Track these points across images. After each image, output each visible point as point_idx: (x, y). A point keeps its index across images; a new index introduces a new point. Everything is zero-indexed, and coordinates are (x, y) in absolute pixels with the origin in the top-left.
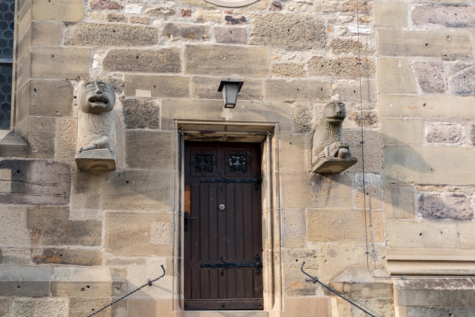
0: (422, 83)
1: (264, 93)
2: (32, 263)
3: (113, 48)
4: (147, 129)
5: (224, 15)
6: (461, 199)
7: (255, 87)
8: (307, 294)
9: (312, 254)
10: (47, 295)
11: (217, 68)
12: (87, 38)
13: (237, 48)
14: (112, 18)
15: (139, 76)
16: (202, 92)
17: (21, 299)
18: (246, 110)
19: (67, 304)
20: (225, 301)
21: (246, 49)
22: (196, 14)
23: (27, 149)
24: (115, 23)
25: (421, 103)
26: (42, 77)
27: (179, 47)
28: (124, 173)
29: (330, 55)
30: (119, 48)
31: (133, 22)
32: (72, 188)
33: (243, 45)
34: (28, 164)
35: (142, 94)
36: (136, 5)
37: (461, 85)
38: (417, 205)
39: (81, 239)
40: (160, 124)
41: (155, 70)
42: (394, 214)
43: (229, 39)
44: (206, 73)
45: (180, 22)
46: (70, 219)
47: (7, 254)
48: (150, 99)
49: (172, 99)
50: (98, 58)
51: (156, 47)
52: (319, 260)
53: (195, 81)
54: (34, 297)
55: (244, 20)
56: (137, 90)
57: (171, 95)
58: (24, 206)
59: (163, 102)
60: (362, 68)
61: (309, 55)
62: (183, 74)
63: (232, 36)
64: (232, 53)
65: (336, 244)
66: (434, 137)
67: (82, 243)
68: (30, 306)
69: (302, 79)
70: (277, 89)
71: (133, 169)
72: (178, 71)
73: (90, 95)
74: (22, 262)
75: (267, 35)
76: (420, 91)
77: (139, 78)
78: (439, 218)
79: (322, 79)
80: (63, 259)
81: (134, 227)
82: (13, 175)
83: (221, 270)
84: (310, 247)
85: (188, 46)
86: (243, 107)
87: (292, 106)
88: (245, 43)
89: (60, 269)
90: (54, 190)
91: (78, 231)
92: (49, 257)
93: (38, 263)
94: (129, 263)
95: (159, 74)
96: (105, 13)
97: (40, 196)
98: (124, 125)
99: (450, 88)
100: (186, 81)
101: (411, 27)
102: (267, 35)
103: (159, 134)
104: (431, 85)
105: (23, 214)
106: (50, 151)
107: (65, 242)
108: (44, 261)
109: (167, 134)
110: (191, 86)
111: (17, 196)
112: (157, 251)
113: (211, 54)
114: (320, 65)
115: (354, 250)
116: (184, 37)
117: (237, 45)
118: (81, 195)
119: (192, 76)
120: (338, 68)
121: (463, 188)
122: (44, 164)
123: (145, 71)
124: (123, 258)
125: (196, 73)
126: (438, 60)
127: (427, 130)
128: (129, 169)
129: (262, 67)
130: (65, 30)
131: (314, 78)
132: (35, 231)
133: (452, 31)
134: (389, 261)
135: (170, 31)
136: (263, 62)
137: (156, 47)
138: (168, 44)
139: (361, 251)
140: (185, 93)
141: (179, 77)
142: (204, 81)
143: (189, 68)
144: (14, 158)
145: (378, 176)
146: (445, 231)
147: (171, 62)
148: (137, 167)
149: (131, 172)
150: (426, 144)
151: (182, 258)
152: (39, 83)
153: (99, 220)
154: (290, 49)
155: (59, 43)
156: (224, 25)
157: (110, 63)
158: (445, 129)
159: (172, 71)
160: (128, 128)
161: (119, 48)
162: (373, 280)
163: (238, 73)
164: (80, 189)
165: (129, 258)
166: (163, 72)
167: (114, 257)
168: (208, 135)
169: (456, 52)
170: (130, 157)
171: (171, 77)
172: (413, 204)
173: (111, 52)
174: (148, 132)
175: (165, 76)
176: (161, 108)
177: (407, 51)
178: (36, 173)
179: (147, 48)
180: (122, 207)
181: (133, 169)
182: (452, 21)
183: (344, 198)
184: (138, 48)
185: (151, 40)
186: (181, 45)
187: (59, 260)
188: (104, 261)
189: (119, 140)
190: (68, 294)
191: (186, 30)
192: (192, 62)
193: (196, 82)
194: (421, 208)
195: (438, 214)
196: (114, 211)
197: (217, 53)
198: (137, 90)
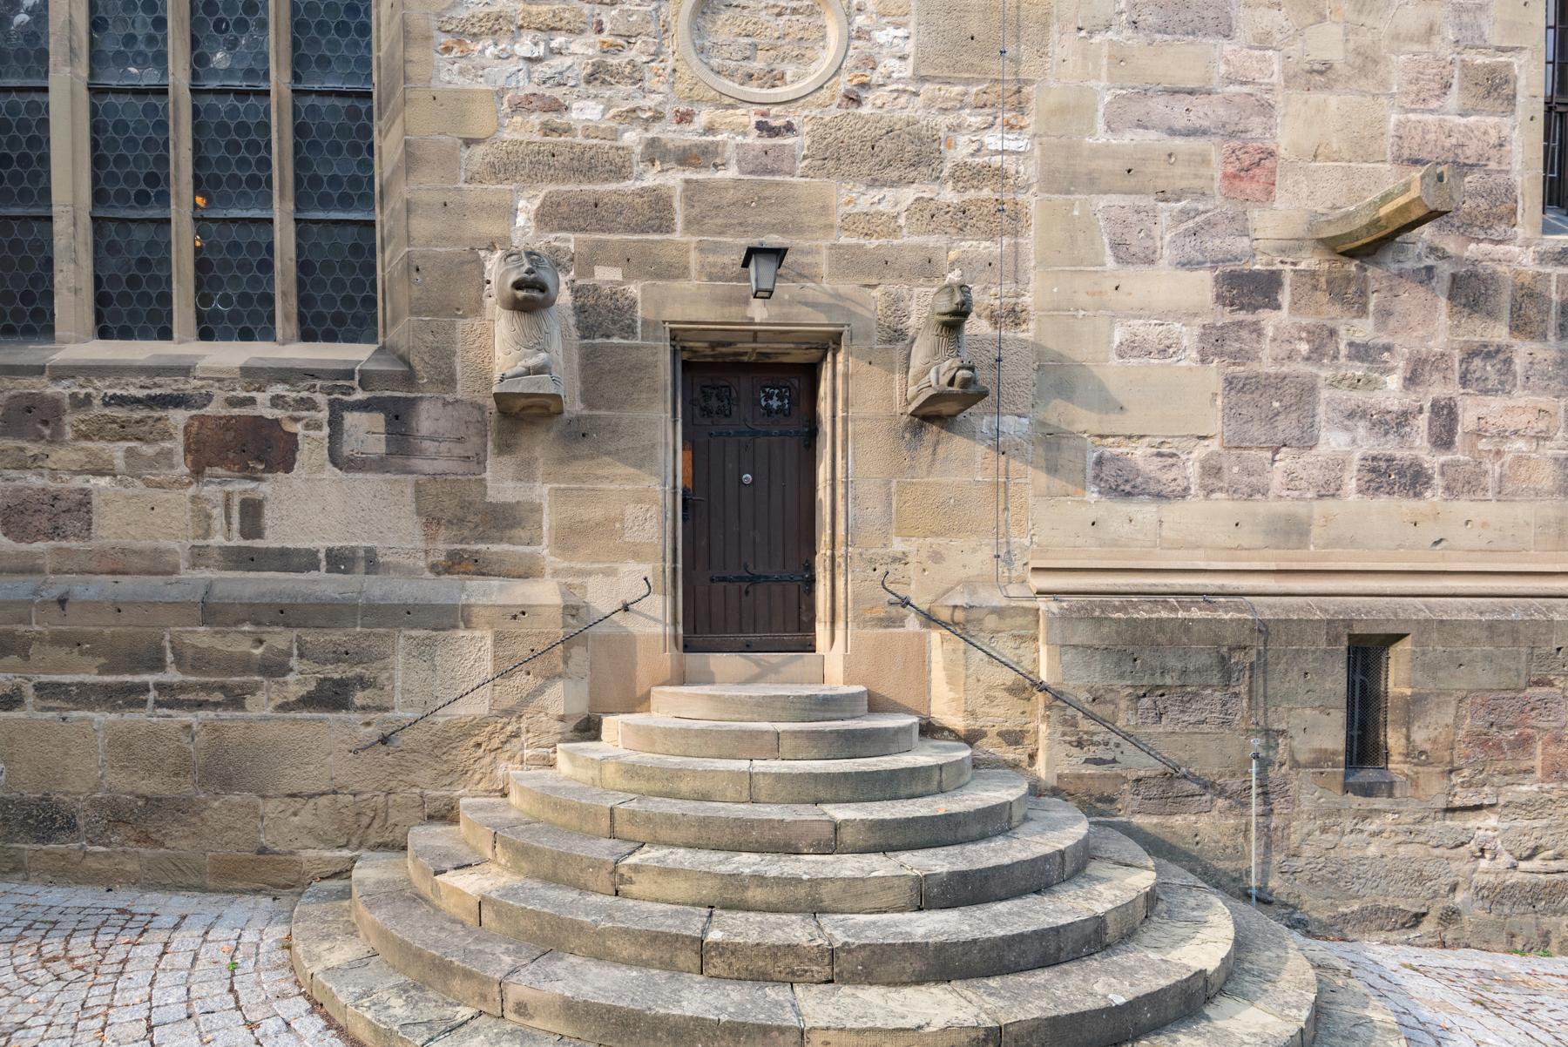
0: (1116, 245)
1: (824, 270)
2: (428, 574)
3: (552, 187)
4: (615, 340)
5: (754, 119)
6: (1170, 461)
9: (902, 559)
10: (455, 627)
11: (740, 224)
12: (505, 168)
13: (778, 184)
14: (548, 129)
15: (600, 241)
16: (714, 270)
17: (414, 633)
18: (791, 302)
19: (489, 642)
20: (752, 637)
21: (793, 186)
22: (703, 117)
23: (409, 378)
24: (554, 138)
25: (1109, 285)
26: (428, 243)
27: (671, 183)
28: (578, 419)
29: (949, 195)
30: (563, 188)
31: (587, 137)
32: (490, 446)
33: (788, 179)
34: (411, 403)
35: (606, 275)
36: (591, 103)
37: (1188, 249)
38: (1090, 473)
39: (508, 533)
40: (639, 330)
41: (628, 228)
43: (763, 165)
44: (721, 233)
45: (671, 134)
46: (488, 500)
47: (386, 559)
48: (620, 284)
50: (527, 207)
51: (630, 185)
52: (912, 570)
53: (701, 249)
54: (435, 629)
55: (789, 128)
56: (596, 268)
57: (658, 276)
58: (410, 477)
59: (643, 290)
60: (1008, 219)
61: (908, 195)
62: (677, 236)
63: (768, 161)
64: (767, 193)
65: (943, 541)
66: (1130, 348)
67: (510, 541)
68: (430, 644)
69: (895, 242)
70: (849, 261)
73: (513, 277)
74: (412, 573)
75: (834, 156)
76: (1110, 262)
77: (601, 245)
78: (1129, 494)
79: (932, 241)
80: (480, 567)
81: (597, 513)
82: (388, 423)
84: (898, 546)
85: (687, 181)
87: (876, 293)
88: (792, 174)
89: (475, 584)
90: (458, 450)
91: (503, 520)
92: (455, 564)
93: (438, 574)
94: (589, 574)
95: (636, 237)
96: (536, 119)
97: (435, 460)
98: (575, 333)
99: (1167, 254)
100: (683, 250)
101: (1101, 137)
102: (834, 156)
103: (638, 348)
104: (1132, 250)
105: (409, 491)
106: (449, 381)
107: (482, 539)
108: (448, 570)
110: (694, 258)
111: (397, 460)
112: (636, 554)
113: (730, 195)
114: (927, 214)
115: (974, 551)
116: (681, 165)
117: (777, 178)
118: (506, 459)
121: (1176, 442)
122: (440, 404)
123: (610, 231)
124: (579, 566)
125: (702, 233)
126: (1147, 201)
127: (1118, 335)
128: (585, 412)
129: (822, 221)
130: (465, 153)
132: (431, 521)
133: (1179, 142)
134: (1034, 569)
135: (655, 152)
136: (825, 209)
137: (630, 185)
138: (652, 178)
139: (986, 553)
140: (681, 272)
141: (671, 242)
142: (716, 248)
143: (689, 223)
144: (388, 393)
145: (1024, 420)
146: (1138, 517)
147: (657, 213)
148: (599, 408)
149: (591, 417)
150: (1115, 361)
151: (680, 566)
152: (423, 256)
154: (874, 183)
155: (455, 180)
156: (754, 139)
157: (548, 216)
158: (1150, 332)
159: (659, 230)
160: (583, 337)
161: (563, 188)
162: (1004, 603)
163: (778, 232)
164: (504, 448)
165: (589, 567)
166: (642, 232)
167: (566, 564)
168: (724, 350)
169: (1184, 184)
170: (587, 390)
172: (1084, 470)
173: (549, 195)
174: (618, 346)
175: (647, 241)
177: (1093, 184)
178: (427, 420)
179: (613, 186)
180: (575, 478)
182: (1181, 123)
183: (962, 461)
184: (597, 188)
185: (619, 171)
186: (675, 179)
187: (472, 568)
188: (548, 570)
189: (568, 360)
190: (491, 624)
191: (685, 150)
193: (702, 250)
194: (1096, 477)
195: (1128, 488)
197: (740, 195)
198: (596, 268)
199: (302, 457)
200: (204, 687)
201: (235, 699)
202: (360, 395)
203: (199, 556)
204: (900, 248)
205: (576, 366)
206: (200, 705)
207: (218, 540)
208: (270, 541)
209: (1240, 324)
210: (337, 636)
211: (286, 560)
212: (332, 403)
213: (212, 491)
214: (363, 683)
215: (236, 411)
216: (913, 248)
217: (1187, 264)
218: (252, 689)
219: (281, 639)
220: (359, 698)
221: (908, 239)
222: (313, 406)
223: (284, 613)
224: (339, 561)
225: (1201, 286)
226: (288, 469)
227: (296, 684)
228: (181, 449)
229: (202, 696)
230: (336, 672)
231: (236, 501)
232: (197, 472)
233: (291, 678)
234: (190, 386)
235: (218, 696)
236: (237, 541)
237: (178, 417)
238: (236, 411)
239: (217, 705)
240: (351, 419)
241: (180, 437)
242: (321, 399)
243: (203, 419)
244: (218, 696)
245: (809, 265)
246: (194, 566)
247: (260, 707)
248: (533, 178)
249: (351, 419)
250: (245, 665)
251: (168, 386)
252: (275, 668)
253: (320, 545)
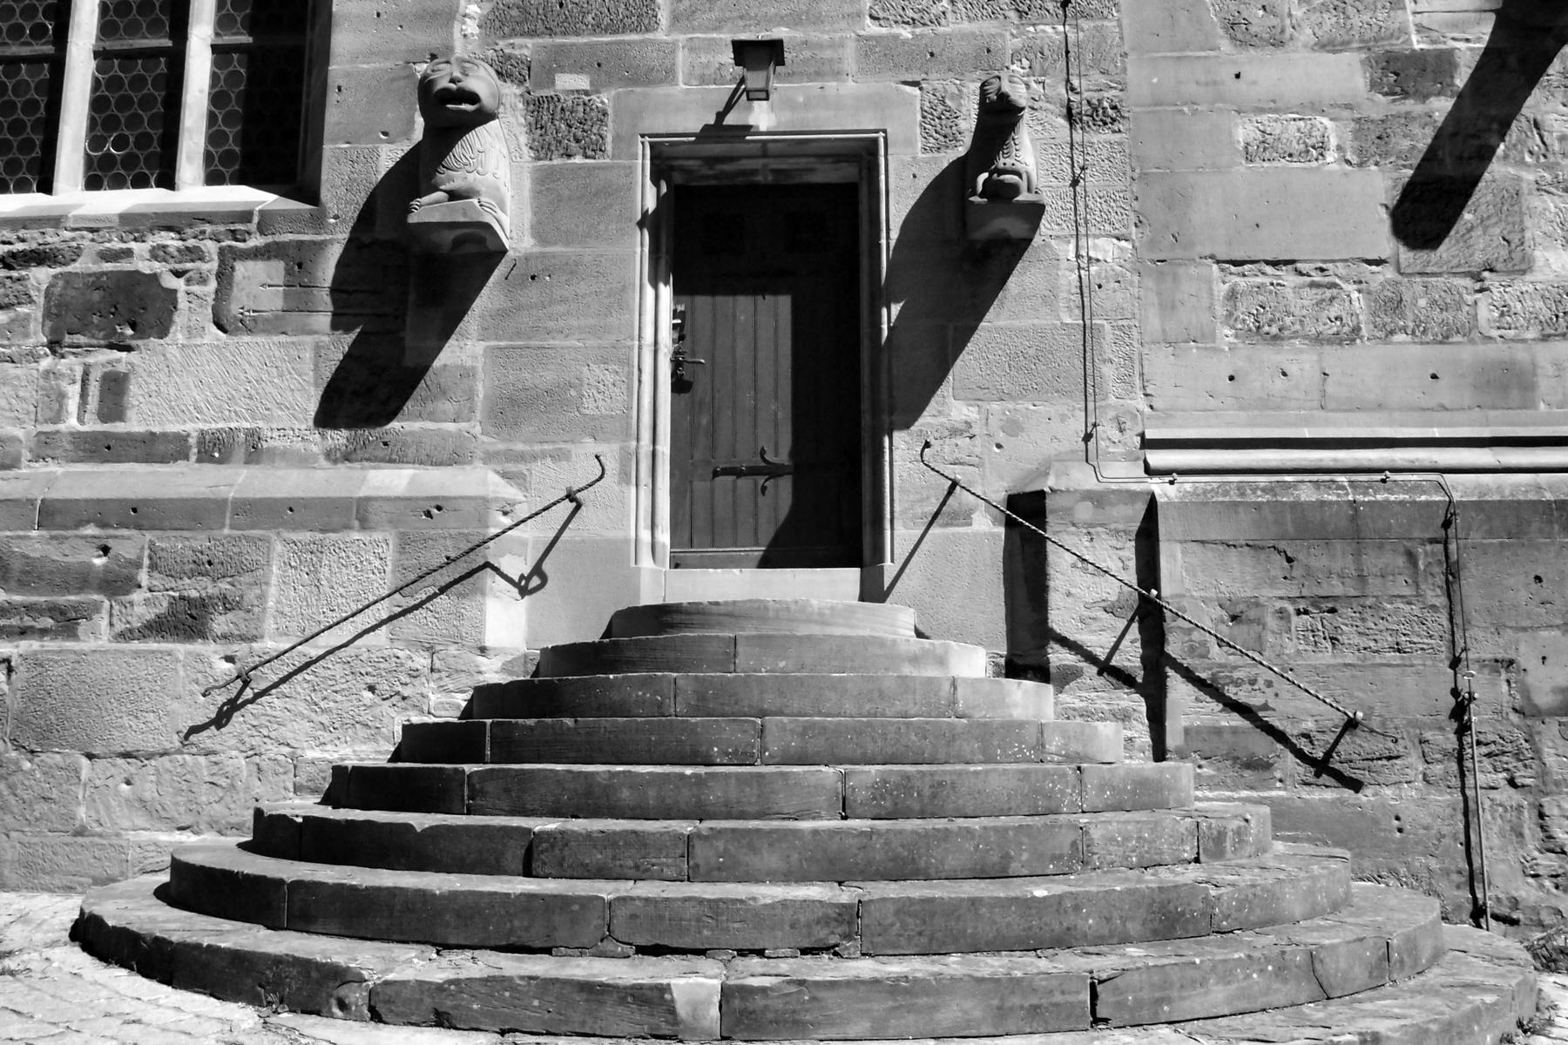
2: (323, 461)
4: (578, 160)
6: (1329, 293)
7: (828, 54)
8: (952, 525)
11: (741, 18)
15: (564, 45)
16: (707, 72)
17: (294, 536)
18: (806, 106)
25: (1227, 73)
28: (527, 258)
32: (412, 297)
35: (569, 82)
37: (1326, 27)
38: (1221, 311)
39: (430, 406)
40: (609, 148)
41: (597, 28)
42: (1164, 331)
44: (715, 29)
47: (272, 443)
48: (587, 93)
49: (638, 90)
53: (692, 48)
54: (323, 531)
57: (634, 81)
58: (308, 339)
59: (617, 98)
62: (660, 35)
66: (1264, 148)
67: (432, 417)
68: (317, 550)
69: (941, 29)
71: (548, 249)
76: (1225, 45)
78: (1275, 337)
79: (987, 26)
81: (547, 377)
82: (289, 272)
83: (761, 480)
86: (801, 99)
93: (335, 462)
98: (527, 154)
104: (1253, 29)
105: (308, 355)
109: (625, 167)
115: (1063, 418)
119: (682, 37)
124: (520, 447)
125: (694, 30)
127: (1244, 132)
128: (537, 249)
131: (966, 26)
141: (652, 42)
143: (675, 19)
144: (290, 237)
145: (1123, 243)
146: (1292, 369)
148: (555, 244)
149: (543, 256)
151: (664, 448)
153: (469, 364)
158: (1289, 130)
165: (537, 448)
166: (616, 32)
167: (501, 446)
170: (540, 223)
171: (634, 42)
172: (1211, 308)
174: (580, 167)
175: (621, 42)
176: (610, 111)
180: (519, 334)
181: (548, 249)
187: (380, 453)
188: (479, 453)
189: (517, 186)
192: (682, 7)
193: (691, 50)
194: (1230, 314)
195: (1274, 330)
196: (502, 344)
199: (179, 319)
200: (29, 609)
201: (67, 622)
202: (256, 241)
203: (45, 447)
204: (948, 37)
205: (527, 193)
206: (23, 632)
207: (72, 423)
208: (133, 424)
209: (1408, 116)
210: (200, 540)
211: (153, 448)
212: (222, 252)
213: (71, 364)
214: (228, 604)
215: (108, 267)
216: (964, 36)
217: (1328, 45)
218: (88, 612)
219: (130, 544)
220: (220, 623)
222: (195, 254)
223: (136, 514)
224: (214, 449)
225: (1347, 75)
226: (163, 332)
227: (142, 606)
228: (40, 314)
229: (28, 621)
230: (194, 589)
231: (95, 375)
232: (54, 345)
233: (137, 596)
234: (52, 239)
235: (48, 622)
236: (93, 425)
237: (40, 276)
238: (108, 267)
239: (44, 632)
240: (241, 269)
241: (41, 300)
242: (210, 247)
243: (68, 278)
244: (48, 622)
245: (831, 60)
246: (38, 457)
247: (97, 637)
249: (241, 269)
250: (83, 579)
251: (33, 240)
252: (117, 584)
253: (192, 428)
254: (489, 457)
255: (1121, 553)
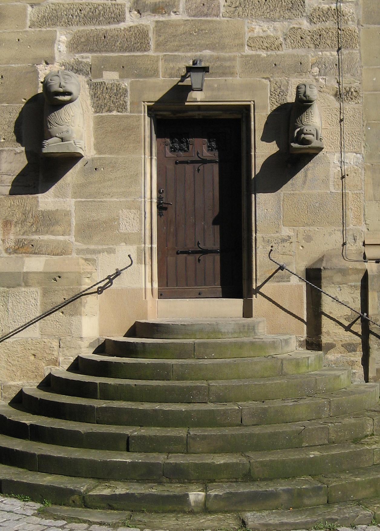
1: (238, 69)
4: (115, 113)
7: (228, 64)
8: (281, 281)
10: (19, 285)
11: (188, 45)
13: (209, 22)
15: (106, 57)
18: (219, 89)
21: (219, 22)
26: (7, 63)
27: (148, 23)
28: (93, 160)
33: (215, 18)
35: (110, 77)
39: (52, 229)
42: (374, 195)
44: (176, 51)
46: (40, 209)
49: (141, 80)
53: (166, 59)
54: (8, 287)
56: (104, 73)
57: (139, 76)
59: (132, 84)
62: (151, 53)
63: (205, 9)
64: (203, 27)
65: (312, 228)
67: (52, 233)
69: (279, 53)
70: (253, 65)
71: (102, 156)
72: (146, 49)
77: (105, 59)
79: (301, 52)
80: (33, 249)
81: (104, 215)
84: (286, 231)
85: (157, 22)
86: (216, 86)
88: (217, 16)
92: (22, 248)
93: (10, 253)
94: (99, 252)
95: (127, 54)
103: (127, 117)
107: (36, 232)
108: (15, 251)
109: (136, 117)
112: (127, 239)
113: (181, 29)
115: (330, 234)
116: (153, 13)
117: (209, 18)
119: (161, 54)
120: (318, 40)
122: (12, 154)
123: (112, 51)
124: (92, 247)
129: (237, 42)
131: (290, 51)
136: (238, 35)
137: (122, 25)
140: (155, 73)
142: (175, 59)
143: (158, 45)
145: (358, 155)
147: (138, 39)
148: (105, 153)
149: (100, 159)
151: (155, 246)
152: (5, 70)
153: (68, 209)
155: (25, 27)
157: (76, 45)
160: (96, 112)
163: (210, 49)
165: (100, 247)
166: (131, 51)
167: (85, 247)
170: (98, 143)
171: (139, 56)
174: (116, 116)
175: (133, 56)
176: (129, 90)
179: (113, 26)
180: (90, 196)
181: (102, 156)
184: (104, 27)
186: (149, 21)
190: (39, 283)
191: (156, 4)
192: (161, 39)
196: (83, 200)
197: (187, 28)
198: (104, 73)
204: (284, 56)
205: (91, 129)
221: (286, 51)
245: (229, 67)
248: (69, 23)
254: (79, 252)
255: (353, 295)
